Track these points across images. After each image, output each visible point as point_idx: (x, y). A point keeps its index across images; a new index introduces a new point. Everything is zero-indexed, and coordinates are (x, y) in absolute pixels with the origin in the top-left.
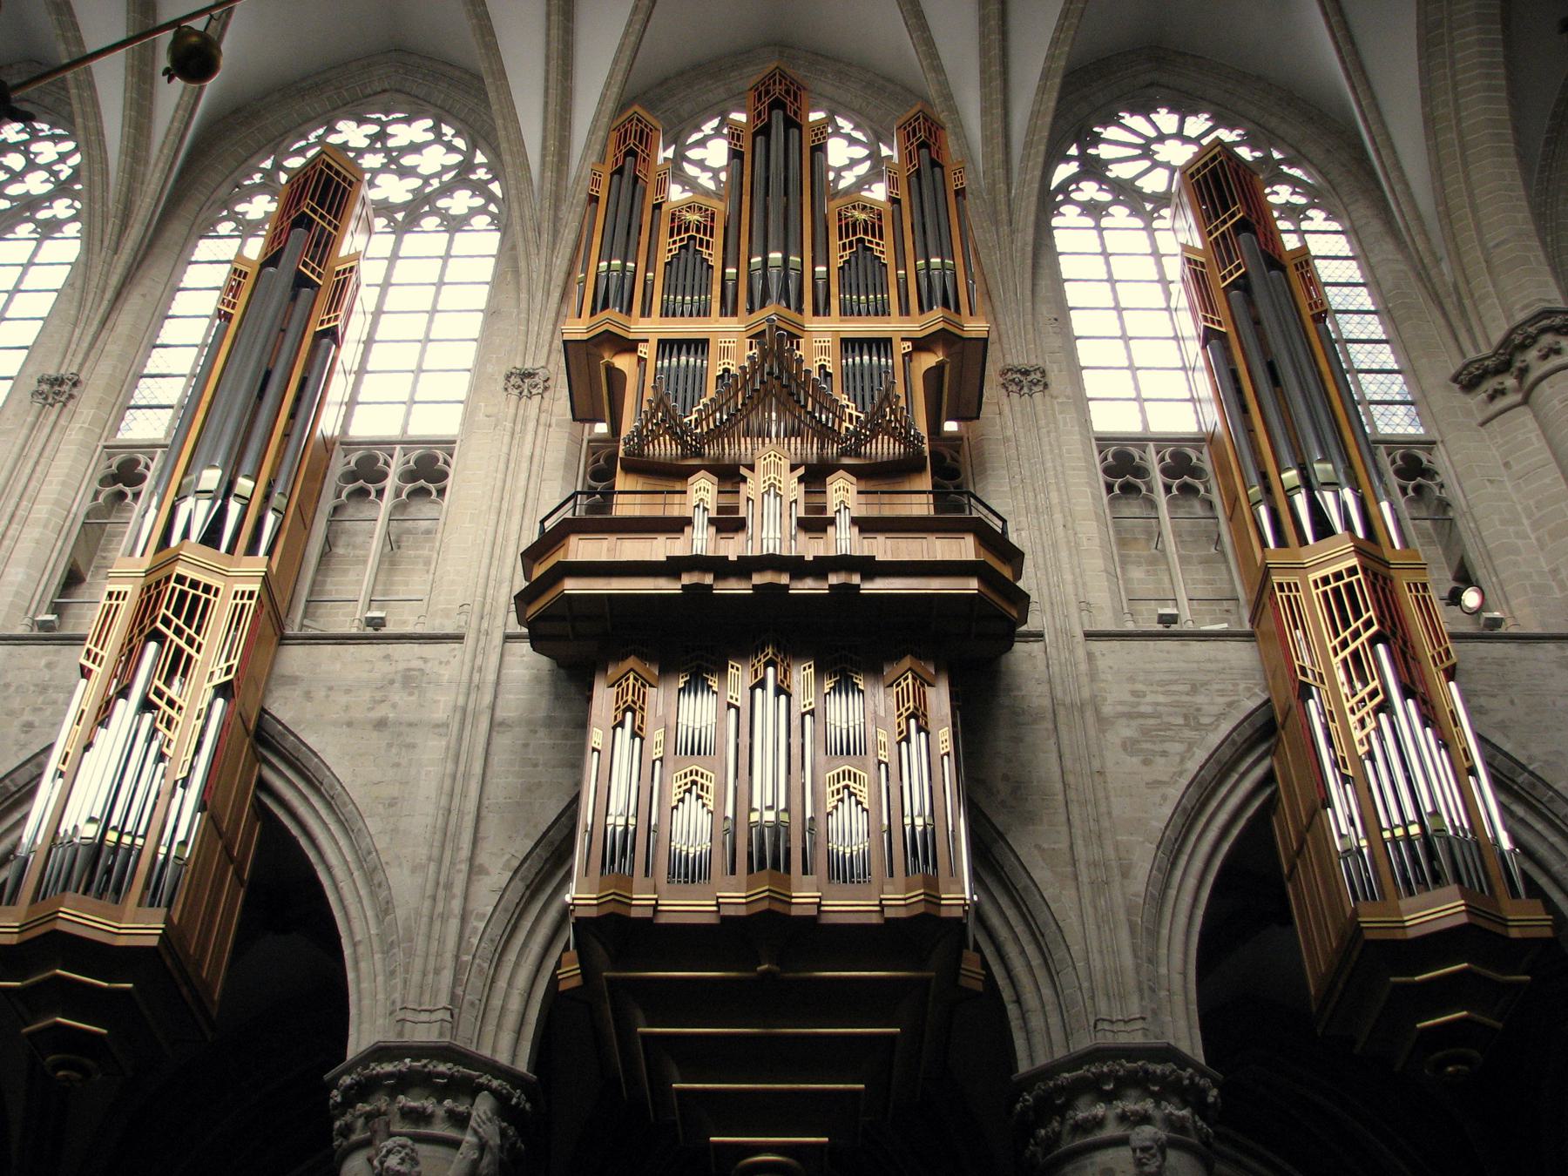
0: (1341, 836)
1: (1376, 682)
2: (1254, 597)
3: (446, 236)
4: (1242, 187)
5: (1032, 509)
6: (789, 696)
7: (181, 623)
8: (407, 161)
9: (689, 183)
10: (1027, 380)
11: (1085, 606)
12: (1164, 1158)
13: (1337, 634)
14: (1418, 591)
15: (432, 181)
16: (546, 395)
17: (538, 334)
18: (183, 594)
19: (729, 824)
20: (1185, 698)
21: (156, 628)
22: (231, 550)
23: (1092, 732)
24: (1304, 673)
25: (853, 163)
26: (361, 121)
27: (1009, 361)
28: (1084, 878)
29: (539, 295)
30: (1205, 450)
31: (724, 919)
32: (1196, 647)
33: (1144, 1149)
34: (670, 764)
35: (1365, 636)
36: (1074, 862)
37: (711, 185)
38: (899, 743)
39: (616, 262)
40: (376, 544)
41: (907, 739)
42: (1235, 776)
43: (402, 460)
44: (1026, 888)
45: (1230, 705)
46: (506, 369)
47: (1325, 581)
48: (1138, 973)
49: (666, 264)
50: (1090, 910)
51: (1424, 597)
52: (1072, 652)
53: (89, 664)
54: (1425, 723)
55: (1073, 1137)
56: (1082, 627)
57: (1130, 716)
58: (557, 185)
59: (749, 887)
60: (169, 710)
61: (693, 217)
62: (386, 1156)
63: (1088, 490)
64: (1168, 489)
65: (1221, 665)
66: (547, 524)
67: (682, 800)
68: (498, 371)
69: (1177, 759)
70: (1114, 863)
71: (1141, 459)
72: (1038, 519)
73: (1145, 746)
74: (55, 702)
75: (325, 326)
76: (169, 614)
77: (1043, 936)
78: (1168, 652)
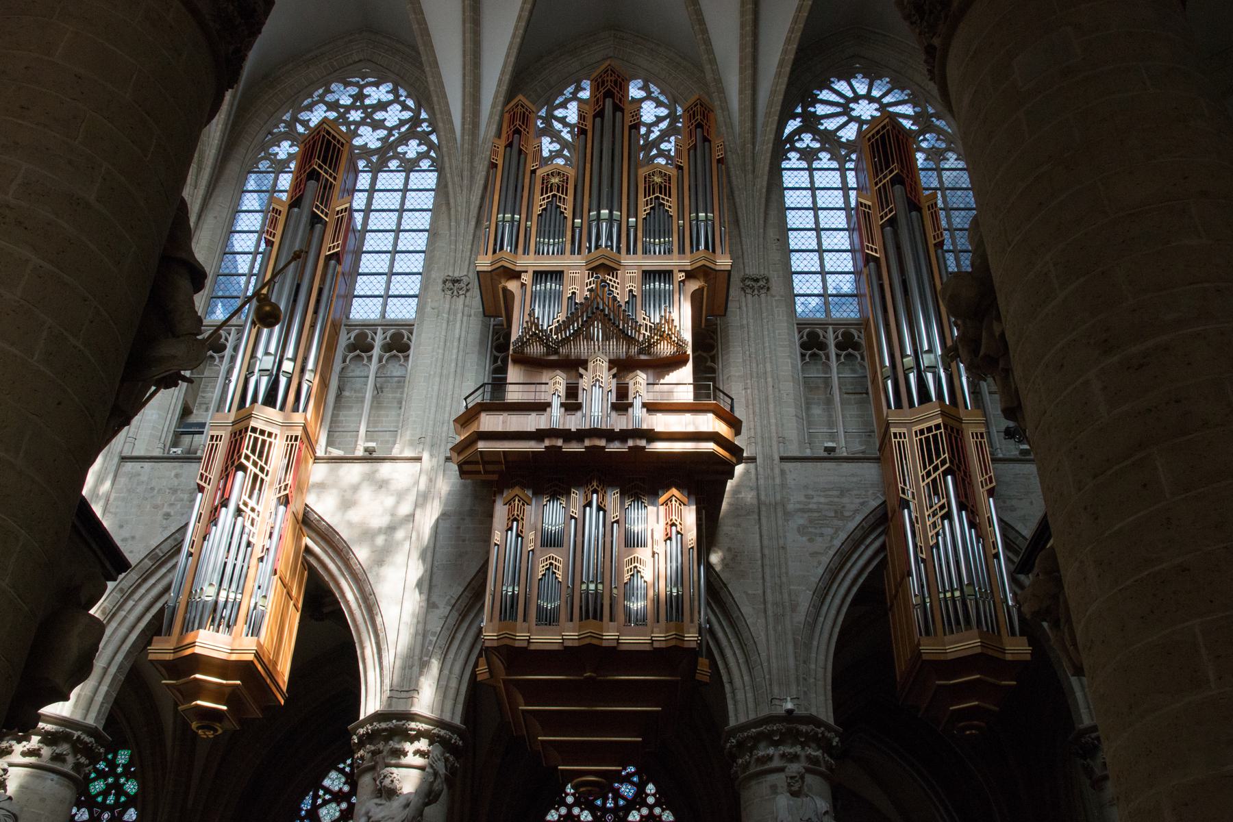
0: (916, 595)
1: (945, 500)
2: (883, 430)
3: (404, 174)
4: (899, 148)
5: (755, 375)
6: (605, 512)
7: (256, 458)
8: (379, 116)
9: (556, 137)
10: (757, 285)
11: (782, 440)
12: (803, 782)
13: (925, 468)
14: (977, 438)
15: (394, 132)
16: (468, 294)
17: (463, 251)
18: (256, 439)
19: (569, 591)
20: (836, 500)
21: (241, 462)
22: (282, 409)
23: (780, 522)
24: (904, 493)
25: (659, 120)
26: (347, 84)
27: (747, 272)
28: (770, 613)
29: (463, 224)
30: (863, 331)
31: (565, 647)
32: (847, 467)
33: (792, 778)
34: (538, 552)
35: (941, 470)
36: (765, 602)
37: (568, 137)
38: (666, 541)
39: (508, 216)
40: (369, 395)
41: (670, 539)
42: (863, 547)
43: (382, 337)
44: (738, 617)
45: (862, 504)
46: (443, 276)
47: (922, 432)
48: (797, 671)
49: (539, 215)
50: (772, 632)
51: (980, 442)
52: (772, 469)
53: (202, 483)
54: (972, 525)
55: (756, 766)
56: (779, 452)
57: (803, 511)
58: (472, 144)
59: (580, 628)
60: (253, 515)
61: (555, 180)
62: (384, 779)
63: (789, 361)
64: (838, 356)
65: (859, 479)
66: (468, 400)
67: (544, 575)
68: (438, 276)
69: (829, 538)
70: (787, 604)
71: (824, 337)
72: (758, 382)
73: (810, 530)
74: (182, 500)
75: (332, 252)
76: (249, 453)
77: (746, 645)
78: (829, 470)
